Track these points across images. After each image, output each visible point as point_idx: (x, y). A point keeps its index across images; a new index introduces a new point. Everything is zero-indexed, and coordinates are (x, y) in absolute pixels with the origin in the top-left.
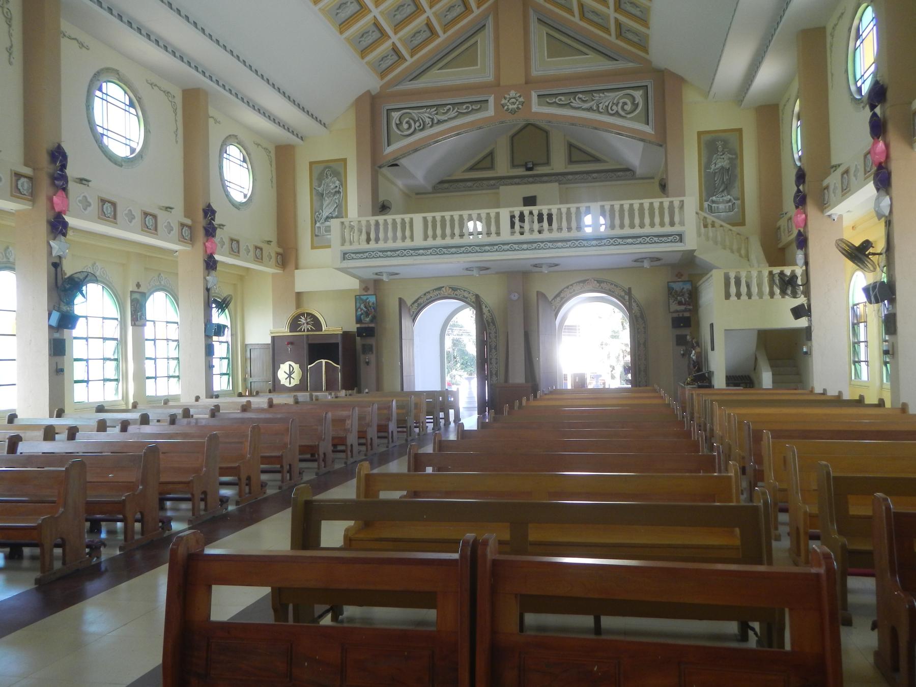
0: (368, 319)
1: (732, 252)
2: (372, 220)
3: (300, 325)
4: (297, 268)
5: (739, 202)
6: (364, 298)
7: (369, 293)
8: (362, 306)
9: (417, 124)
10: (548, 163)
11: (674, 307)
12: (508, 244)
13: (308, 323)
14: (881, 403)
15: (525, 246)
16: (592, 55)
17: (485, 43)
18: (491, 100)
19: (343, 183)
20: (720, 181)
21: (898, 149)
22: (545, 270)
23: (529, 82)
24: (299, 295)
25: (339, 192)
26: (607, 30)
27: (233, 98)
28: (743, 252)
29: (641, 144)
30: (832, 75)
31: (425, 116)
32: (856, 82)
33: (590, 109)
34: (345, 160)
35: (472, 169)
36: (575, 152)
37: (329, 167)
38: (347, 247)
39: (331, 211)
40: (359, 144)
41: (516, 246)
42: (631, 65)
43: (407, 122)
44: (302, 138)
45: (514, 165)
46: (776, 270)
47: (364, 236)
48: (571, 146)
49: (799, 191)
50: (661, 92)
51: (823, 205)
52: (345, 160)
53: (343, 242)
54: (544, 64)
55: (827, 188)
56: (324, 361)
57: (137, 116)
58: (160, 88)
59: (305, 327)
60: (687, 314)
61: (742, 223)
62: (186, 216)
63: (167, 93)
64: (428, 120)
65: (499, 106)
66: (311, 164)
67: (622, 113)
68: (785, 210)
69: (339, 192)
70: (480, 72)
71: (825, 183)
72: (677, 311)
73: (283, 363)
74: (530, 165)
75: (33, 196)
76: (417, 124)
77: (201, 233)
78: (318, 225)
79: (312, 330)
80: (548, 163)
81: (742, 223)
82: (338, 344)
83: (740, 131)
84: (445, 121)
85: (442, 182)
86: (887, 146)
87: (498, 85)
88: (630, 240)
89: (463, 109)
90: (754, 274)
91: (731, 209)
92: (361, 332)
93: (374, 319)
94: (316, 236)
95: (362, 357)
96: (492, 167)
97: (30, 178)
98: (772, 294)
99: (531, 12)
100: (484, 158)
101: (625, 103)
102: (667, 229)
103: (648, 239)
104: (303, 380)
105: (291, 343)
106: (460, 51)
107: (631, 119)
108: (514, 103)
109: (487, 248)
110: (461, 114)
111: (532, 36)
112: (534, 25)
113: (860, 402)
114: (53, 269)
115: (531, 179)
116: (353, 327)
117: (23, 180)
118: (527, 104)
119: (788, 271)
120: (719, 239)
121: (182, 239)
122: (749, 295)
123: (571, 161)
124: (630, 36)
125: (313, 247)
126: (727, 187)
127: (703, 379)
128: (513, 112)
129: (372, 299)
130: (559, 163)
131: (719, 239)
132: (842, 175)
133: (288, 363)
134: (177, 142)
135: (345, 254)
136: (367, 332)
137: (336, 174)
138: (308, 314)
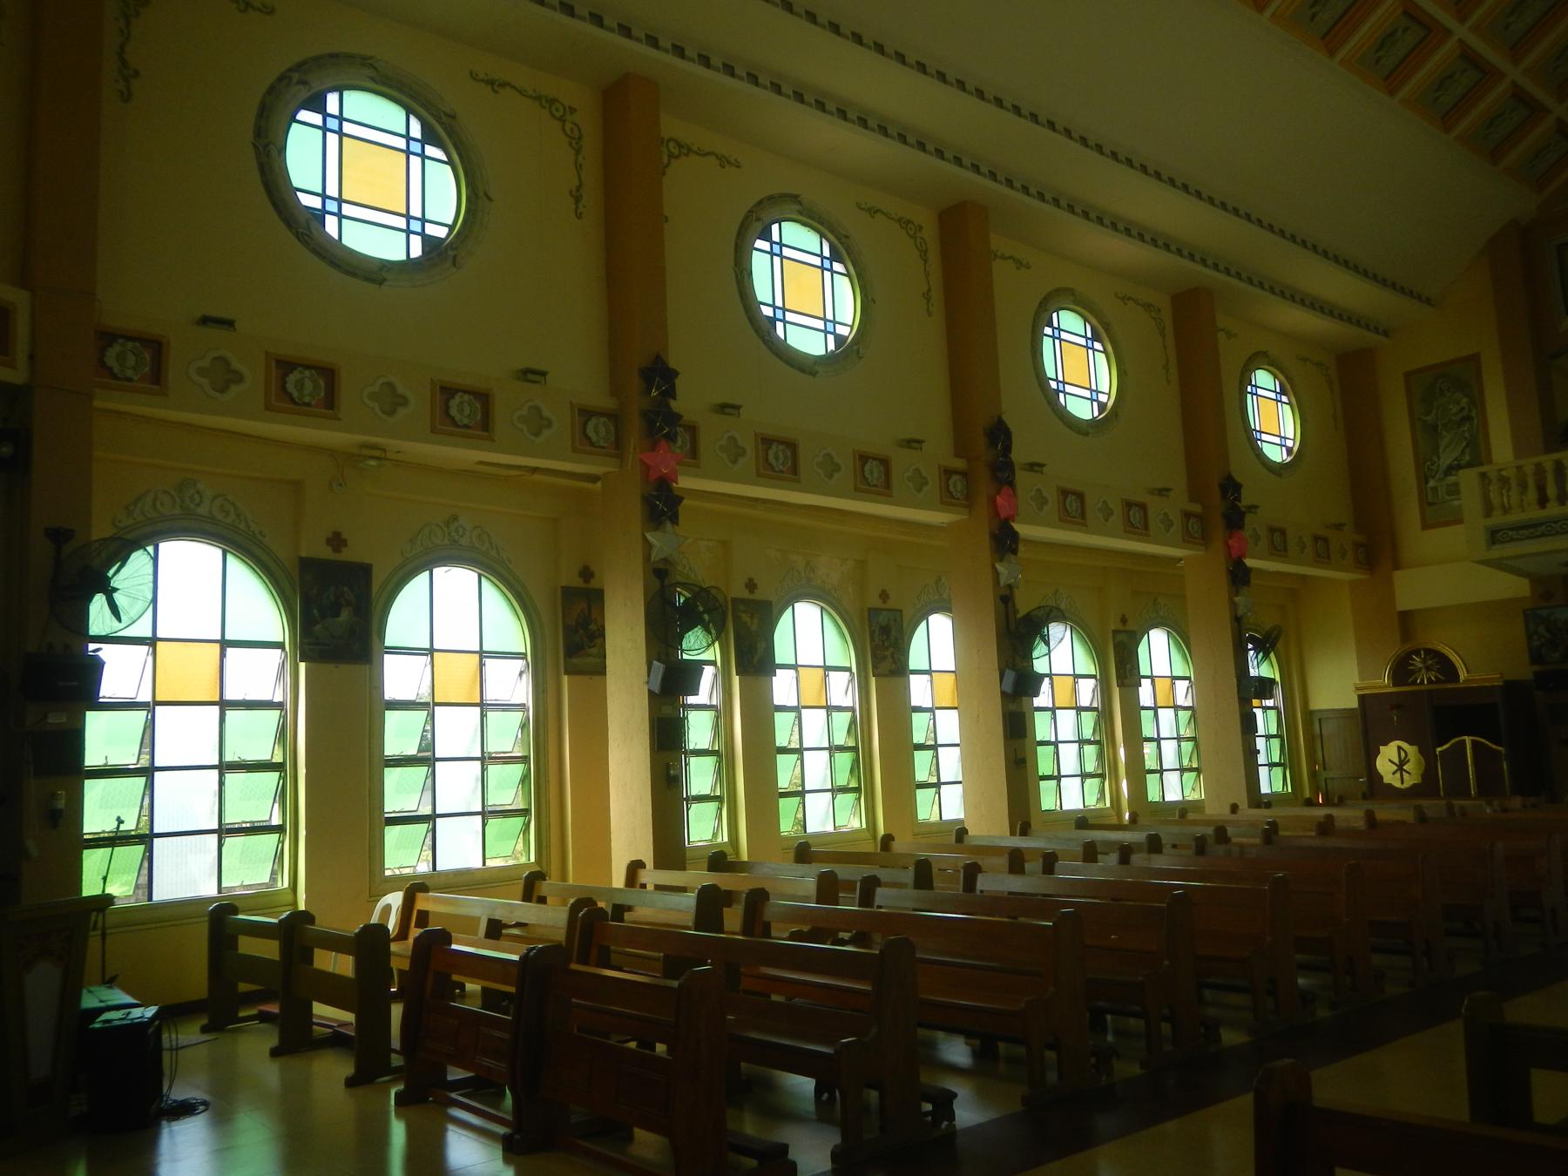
2: (1548, 461)
3: (1412, 672)
4: (1397, 567)
8: (1542, 630)
13: (1428, 669)
19: (1478, 403)
24: (1406, 618)
25: (1468, 418)
27: (1258, 291)
34: (1475, 358)
38: (1498, 519)
39: (1456, 454)
44: (1386, 334)
47: (1532, 495)
52: (1475, 358)
53: (1488, 510)
56: (1468, 740)
57: (1105, 352)
58: (1136, 302)
62: (1192, 499)
63: (1148, 307)
66: (1407, 375)
69: (1468, 418)
73: (1386, 744)
75: (969, 501)
78: (1432, 483)
79: (1438, 681)
94: (1430, 504)
97: (964, 474)
104: (1428, 774)
105: (1399, 707)
114: (1002, 606)
116: (1523, 670)
117: (955, 477)
121: (1188, 539)
125: (1426, 526)
133: (1394, 745)
134: (1168, 381)
138: (1429, 652)
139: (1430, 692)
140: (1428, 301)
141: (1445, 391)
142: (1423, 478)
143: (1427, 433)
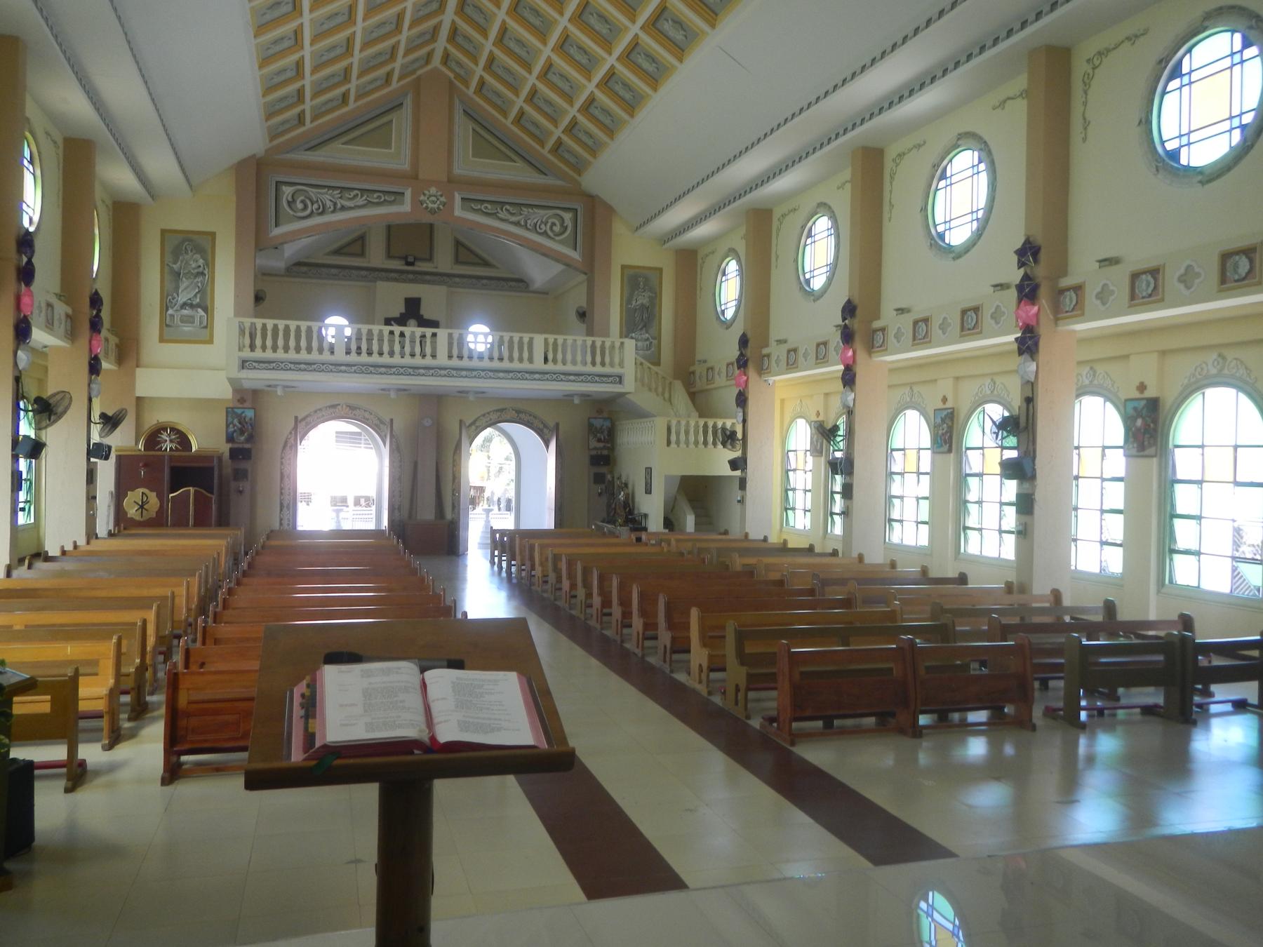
0: (242, 438)
1: (650, 389)
3: (159, 443)
5: (655, 342)
6: (239, 411)
7: (247, 405)
8: (236, 421)
9: (315, 206)
10: (430, 259)
11: (593, 444)
12: (445, 369)
14: (835, 553)
15: (464, 373)
16: (520, 164)
17: (402, 122)
18: (408, 193)
19: (210, 263)
20: (640, 320)
21: (861, 356)
22: (471, 398)
23: (452, 182)
24: (139, 399)
25: (203, 274)
26: (542, 144)
28: (667, 395)
29: (561, 267)
31: (327, 197)
32: (804, 274)
33: (517, 224)
34: (213, 235)
35: (338, 252)
36: (463, 252)
37: (191, 240)
38: (247, 354)
40: (239, 219)
41: (454, 372)
42: (559, 183)
43: (302, 202)
45: (389, 256)
46: (711, 423)
48: (458, 244)
49: (742, 355)
50: (591, 219)
51: (761, 371)
52: (213, 235)
54: (468, 164)
55: (768, 356)
56: (192, 489)
59: (168, 446)
60: (605, 452)
61: (658, 363)
63: (55, 142)
64: (329, 204)
65: (417, 203)
66: (163, 232)
67: (550, 233)
68: (699, 357)
69: (203, 274)
70: (394, 156)
71: (765, 351)
72: (595, 449)
73: (133, 490)
74: (411, 259)
76: (315, 206)
77: (86, 325)
78: (170, 312)
80: (430, 259)
81: (658, 363)
82: (212, 468)
83: (660, 270)
84: (351, 208)
85: (299, 264)
86: (854, 352)
87: (416, 177)
88: (572, 378)
89: (374, 198)
90: (692, 423)
91: (648, 348)
92: (234, 454)
93: (251, 438)
95: (233, 485)
96: (362, 254)
99: (457, 101)
100: (354, 241)
101: (554, 224)
102: (607, 370)
104: (161, 511)
105: (145, 465)
106: (369, 125)
107: (561, 242)
108: (434, 202)
109: (422, 371)
110: (369, 204)
111: (456, 127)
112: (459, 116)
113: (810, 550)
115: (411, 276)
118: (449, 205)
119: (729, 424)
120: (646, 380)
122: (687, 443)
123: (457, 261)
124: (566, 155)
125: (162, 340)
126: (646, 326)
127: (635, 522)
128: (433, 212)
129: (250, 414)
130: (444, 261)
131: (646, 380)
133: (141, 490)
135: (244, 362)
136: (240, 454)
137: (201, 250)
138: (172, 429)
139: (171, 458)
140: (191, 186)
141: (188, 250)
142: (165, 307)
143: (173, 277)
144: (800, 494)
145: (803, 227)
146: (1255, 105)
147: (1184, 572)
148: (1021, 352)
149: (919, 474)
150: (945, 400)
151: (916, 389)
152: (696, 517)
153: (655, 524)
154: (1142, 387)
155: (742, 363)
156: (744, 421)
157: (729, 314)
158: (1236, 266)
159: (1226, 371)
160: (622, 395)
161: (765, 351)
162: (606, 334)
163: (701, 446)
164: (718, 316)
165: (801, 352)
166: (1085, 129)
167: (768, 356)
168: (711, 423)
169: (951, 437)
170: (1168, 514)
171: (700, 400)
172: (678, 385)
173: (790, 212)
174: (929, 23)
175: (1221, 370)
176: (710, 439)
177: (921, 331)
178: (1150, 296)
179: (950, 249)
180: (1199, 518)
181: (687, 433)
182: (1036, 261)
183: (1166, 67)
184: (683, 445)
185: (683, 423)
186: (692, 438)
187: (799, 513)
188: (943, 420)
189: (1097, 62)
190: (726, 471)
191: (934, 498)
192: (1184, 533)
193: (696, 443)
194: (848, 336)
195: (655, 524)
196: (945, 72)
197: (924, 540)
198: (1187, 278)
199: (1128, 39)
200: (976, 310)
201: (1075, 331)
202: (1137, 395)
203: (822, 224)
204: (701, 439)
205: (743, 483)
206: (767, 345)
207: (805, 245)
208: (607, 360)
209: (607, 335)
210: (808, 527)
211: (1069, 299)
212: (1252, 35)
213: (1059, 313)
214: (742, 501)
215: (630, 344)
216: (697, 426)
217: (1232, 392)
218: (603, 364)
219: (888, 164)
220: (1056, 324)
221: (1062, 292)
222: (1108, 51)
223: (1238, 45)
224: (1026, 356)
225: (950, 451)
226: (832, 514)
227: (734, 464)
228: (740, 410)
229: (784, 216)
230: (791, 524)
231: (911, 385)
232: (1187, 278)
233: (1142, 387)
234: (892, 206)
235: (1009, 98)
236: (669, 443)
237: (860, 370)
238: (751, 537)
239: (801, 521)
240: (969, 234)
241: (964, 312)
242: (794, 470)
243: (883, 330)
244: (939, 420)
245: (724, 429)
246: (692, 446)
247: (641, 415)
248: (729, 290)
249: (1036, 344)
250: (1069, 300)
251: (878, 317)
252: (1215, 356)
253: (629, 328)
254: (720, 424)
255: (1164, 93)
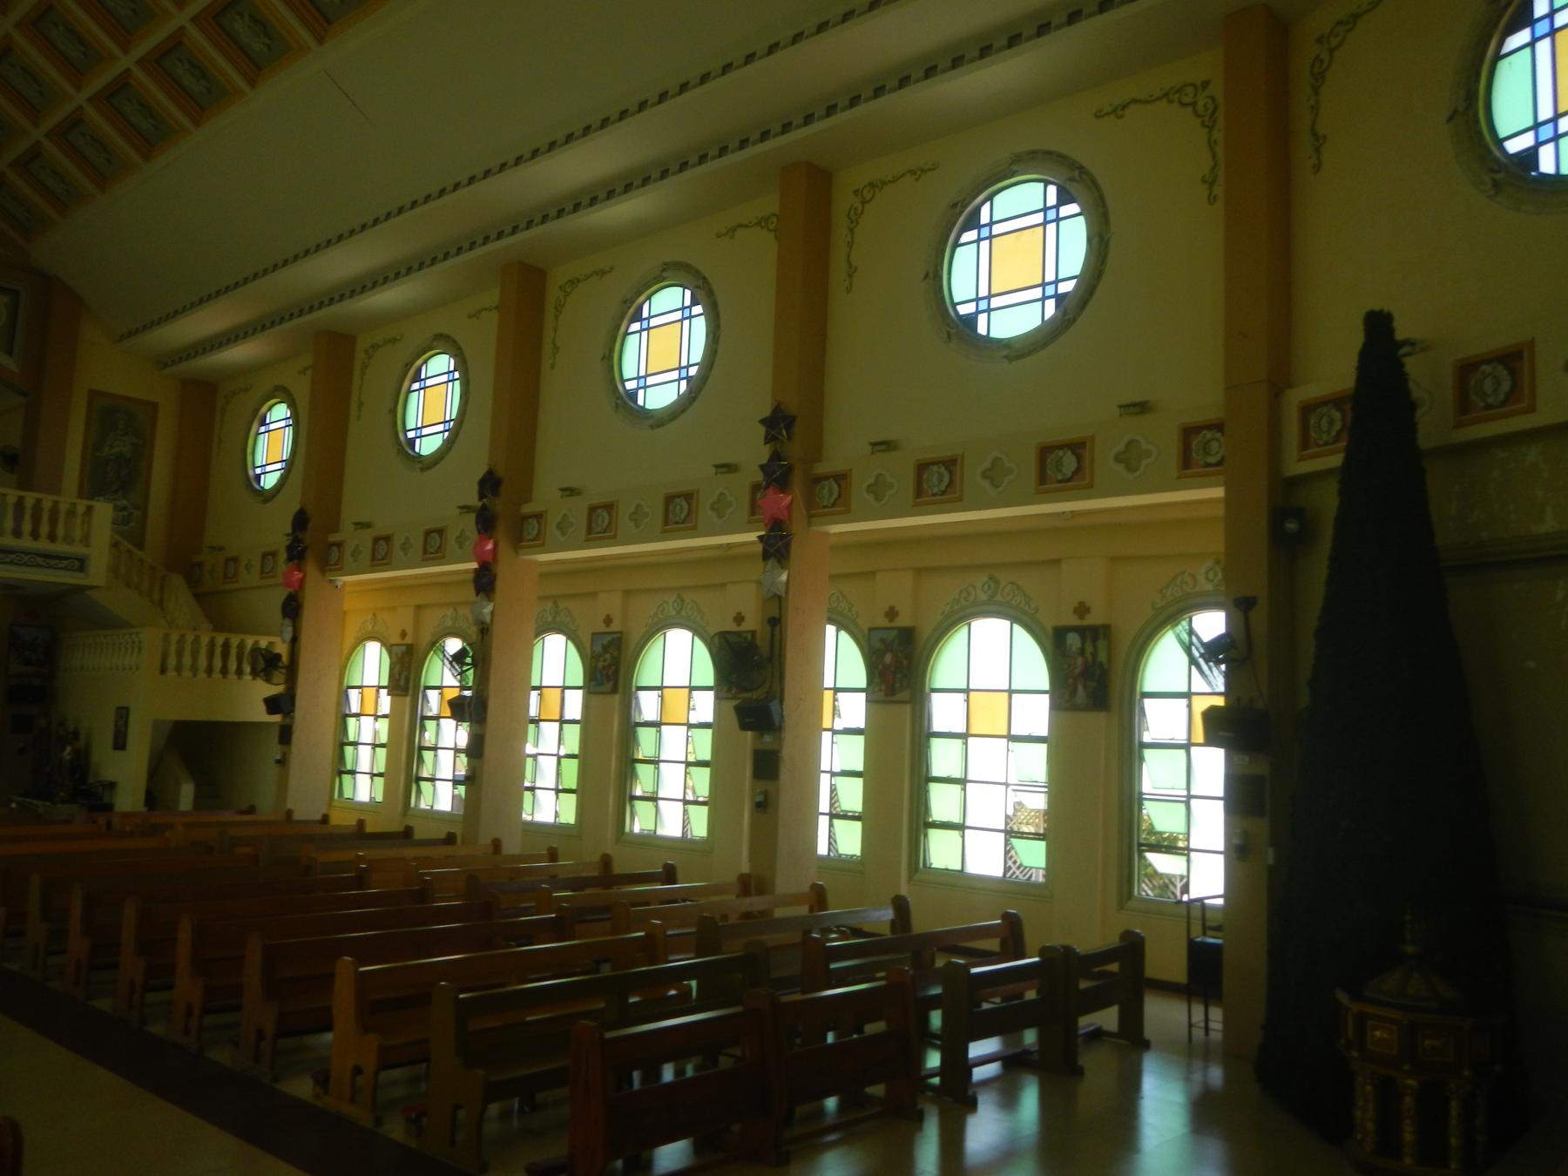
14: (450, 839)
21: (505, 551)
28: (156, 596)
30: (361, 404)
32: (406, 431)
61: (141, 546)
71: (334, 538)
81: (140, 546)
83: (154, 407)
86: (496, 545)
98: (239, 672)
102: (60, 547)
103: (26, 558)
132: (376, 540)
144: (365, 753)
145: (408, 366)
146: (1077, 272)
147: (942, 852)
148: (766, 556)
149: (562, 721)
150: (608, 621)
151: (562, 604)
152: (198, 786)
153: (129, 798)
154: (892, 614)
155: (296, 553)
156: (295, 640)
157: (269, 481)
158: (1059, 465)
159: (999, 598)
160: (80, 589)
161: (334, 538)
162: (55, 488)
163: (217, 675)
164: (250, 483)
165: (398, 541)
166: (850, 276)
167: (339, 545)
168: (235, 641)
169: (616, 672)
170: (921, 778)
171: (217, 608)
172: (177, 581)
173: (387, 342)
174: (663, 97)
175: (992, 597)
176: (233, 666)
177: (601, 521)
178: (944, 493)
179: (644, 413)
180: (962, 782)
181: (195, 654)
182: (790, 438)
183: (960, 215)
184: (187, 674)
185: (190, 638)
186: (203, 662)
187: (363, 782)
188: (605, 649)
189: (868, 197)
190: (260, 714)
191: (585, 757)
192: (942, 803)
193: (210, 670)
194: (486, 522)
195: (129, 798)
196: (664, 174)
197: (569, 816)
198: (993, 474)
199: (912, 172)
200: (689, 497)
201: (828, 534)
202: (885, 623)
203: (440, 364)
204: (218, 663)
205: (286, 735)
206: (335, 528)
207: (409, 391)
208: (61, 531)
209: (58, 492)
210: (379, 798)
211: (828, 491)
212: (1074, 188)
213: (815, 509)
214: (282, 762)
215: (104, 511)
216: (212, 644)
217: (1004, 624)
218: (52, 537)
219: (553, 294)
220: (810, 524)
221: (818, 480)
222: (884, 183)
223: (1052, 199)
224: (772, 562)
225: (614, 690)
226: (419, 779)
227: (273, 704)
228: (288, 622)
229: (375, 347)
230: (347, 794)
231: (555, 599)
232: (993, 474)
233: (892, 614)
234: (556, 348)
235: (741, 226)
236: (163, 671)
237: (503, 571)
238: (297, 816)
239: (364, 790)
240: (674, 397)
241: (669, 499)
242: (357, 715)
243: (539, 516)
244: (598, 649)
245: (256, 650)
246: (202, 675)
247: (106, 622)
248: (272, 446)
249: (787, 546)
250: (833, 493)
251: (528, 500)
252: (985, 579)
253: (94, 486)
254: (250, 642)
255: (957, 245)
